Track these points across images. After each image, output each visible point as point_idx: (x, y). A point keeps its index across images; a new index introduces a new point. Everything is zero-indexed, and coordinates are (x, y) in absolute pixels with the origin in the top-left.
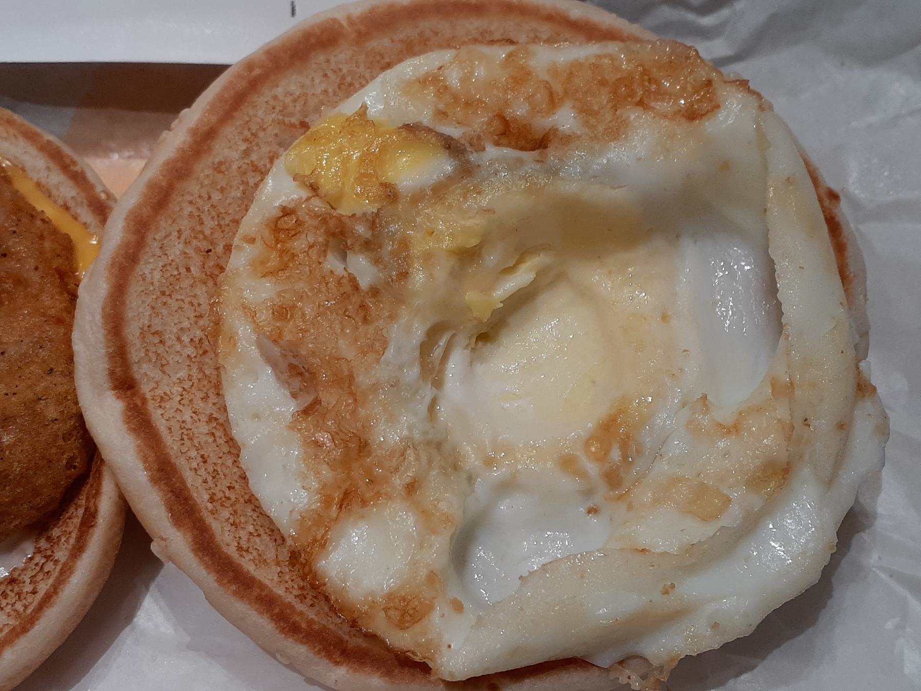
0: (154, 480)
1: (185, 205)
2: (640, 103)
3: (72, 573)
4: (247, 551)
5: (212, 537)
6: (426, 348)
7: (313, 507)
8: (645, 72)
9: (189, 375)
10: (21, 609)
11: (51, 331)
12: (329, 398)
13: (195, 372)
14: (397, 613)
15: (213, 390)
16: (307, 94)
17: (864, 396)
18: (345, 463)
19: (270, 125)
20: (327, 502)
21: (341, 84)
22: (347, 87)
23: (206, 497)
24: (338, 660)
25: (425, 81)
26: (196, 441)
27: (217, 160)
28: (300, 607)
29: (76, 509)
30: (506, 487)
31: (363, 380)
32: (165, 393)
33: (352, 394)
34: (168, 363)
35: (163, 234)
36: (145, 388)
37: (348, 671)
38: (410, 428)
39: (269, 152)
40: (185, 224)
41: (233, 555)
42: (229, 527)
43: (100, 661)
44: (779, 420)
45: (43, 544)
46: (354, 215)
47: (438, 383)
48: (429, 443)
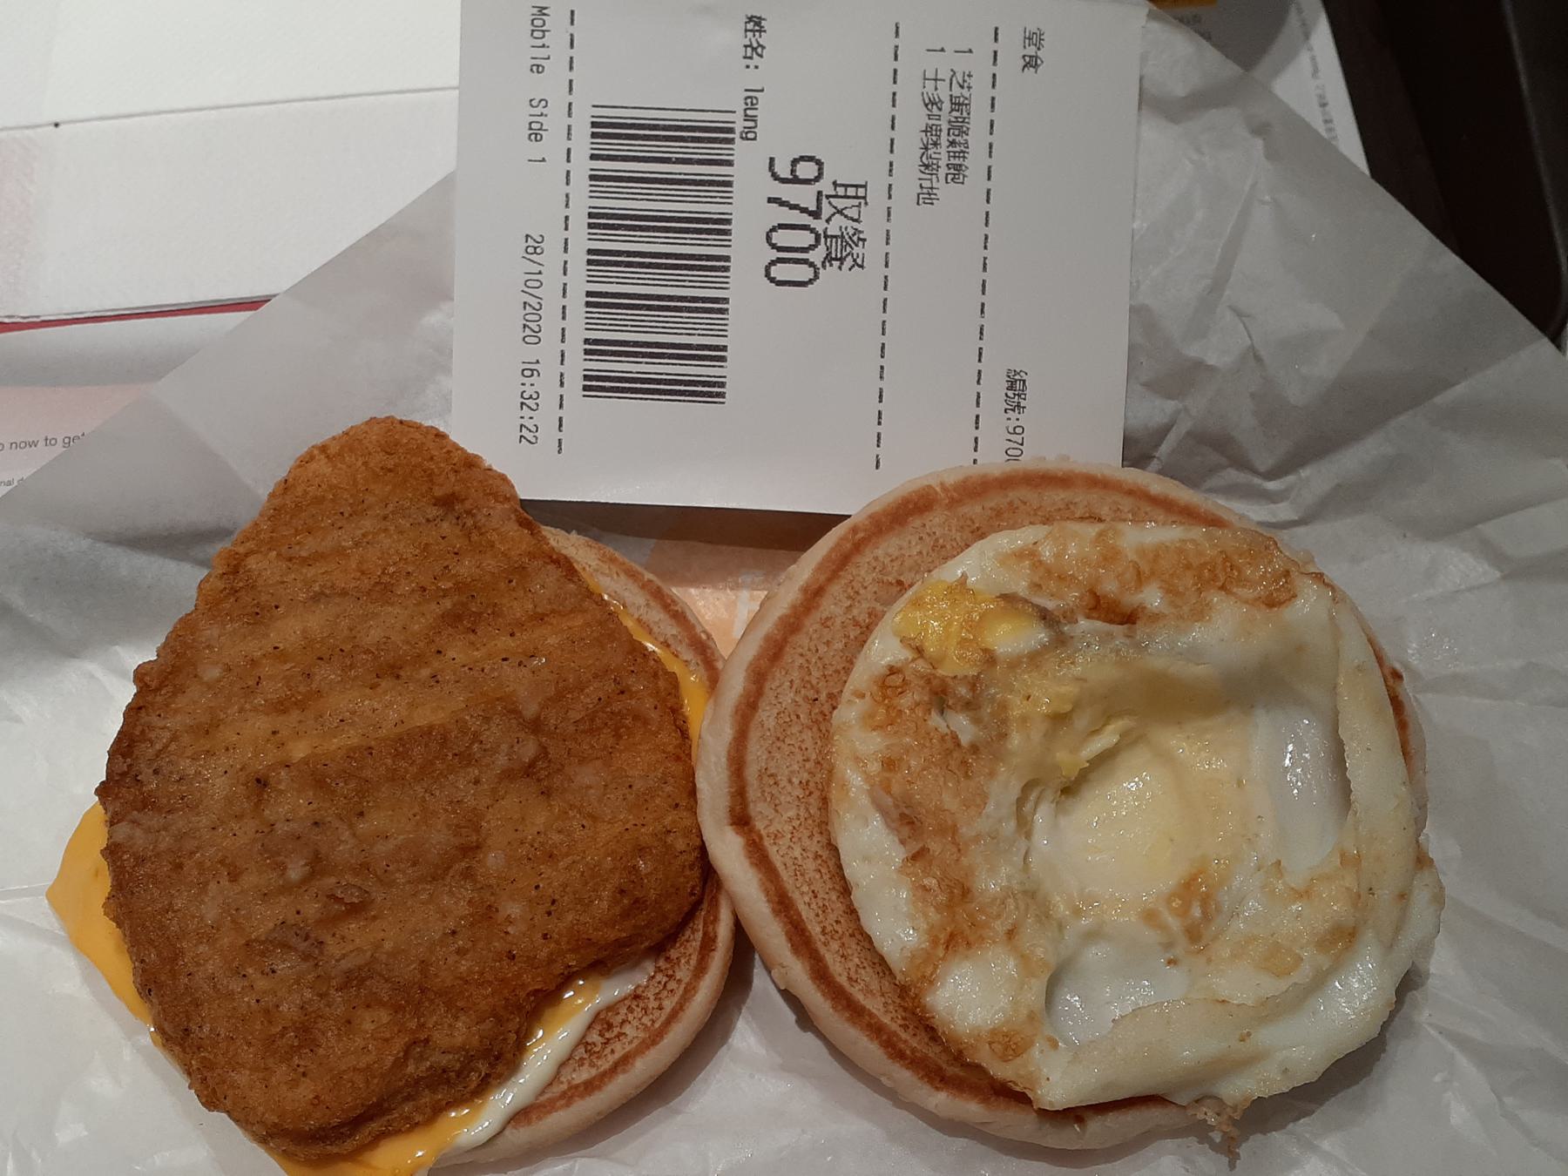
0: (776, 912)
1: (797, 656)
2: (1223, 588)
3: (696, 992)
4: (856, 981)
5: (826, 967)
6: (1021, 802)
7: (923, 946)
8: (1227, 559)
9: (798, 815)
10: (649, 1024)
11: (676, 768)
12: (935, 846)
13: (802, 813)
14: (1000, 1046)
15: (816, 829)
16: (904, 555)
17: (1422, 868)
18: (950, 906)
19: (871, 583)
20: (935, 942)
21: (934, 546)
22: (944, 552)
23: (818, 929)
24: (938, 1086)
25: (1020, 555)
26: (807, 877)
27: (824, 616)
28: (904, 1036)
29: (693, 933)
30: (1092, 936)
31: (966, 831)
32: (778, 831)
33: (955, 843)
34: (781, 804)
35: (777, 683)
36: (759, 825)
37: (948, 1096)
38: (1009, 878)
39: (869, 608)
40: (795, 675)
41: (845, 984)
42: (839, 959)
43: (700, 1076)
44: (1347, 889)
45: (662, 963)
46: (955, 677)
47: (1028, 835)
48: (1025, 892)
